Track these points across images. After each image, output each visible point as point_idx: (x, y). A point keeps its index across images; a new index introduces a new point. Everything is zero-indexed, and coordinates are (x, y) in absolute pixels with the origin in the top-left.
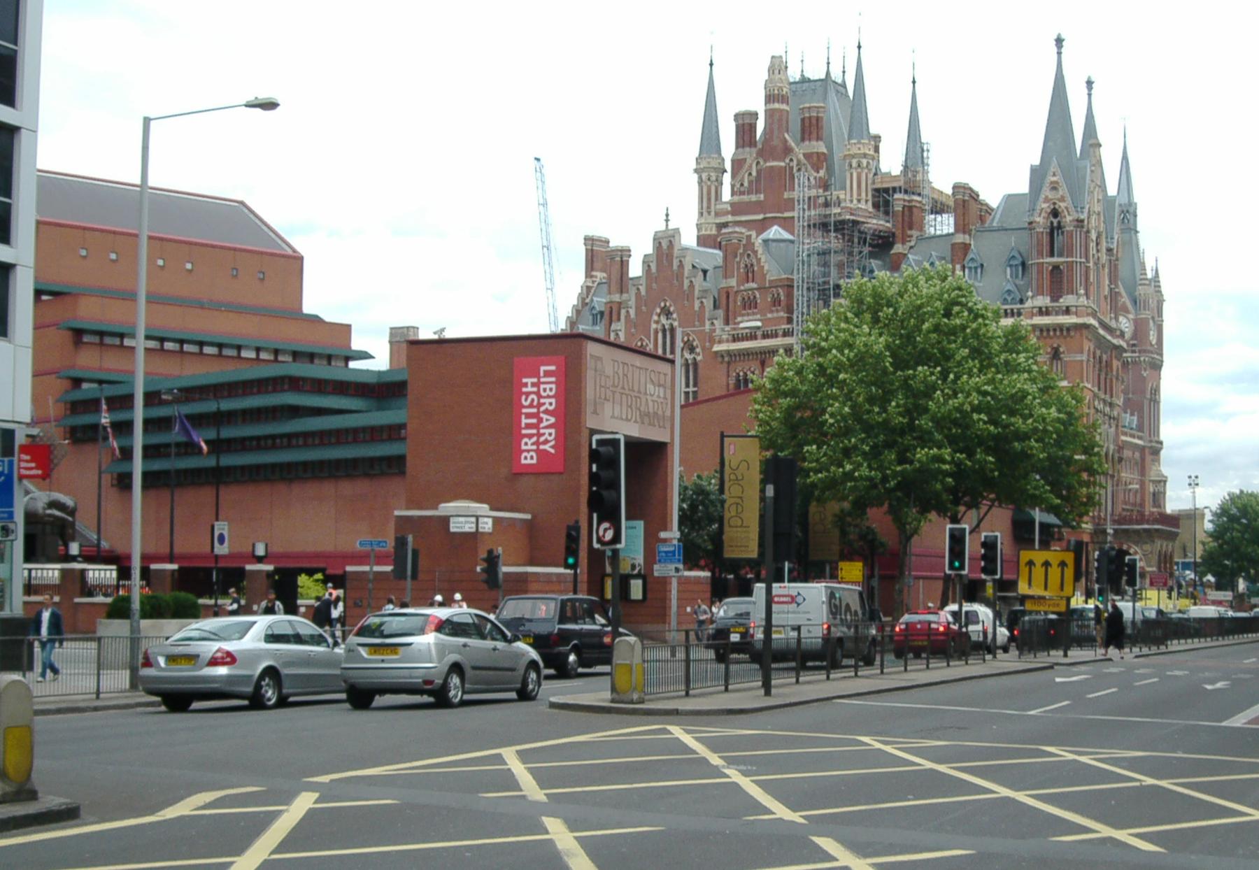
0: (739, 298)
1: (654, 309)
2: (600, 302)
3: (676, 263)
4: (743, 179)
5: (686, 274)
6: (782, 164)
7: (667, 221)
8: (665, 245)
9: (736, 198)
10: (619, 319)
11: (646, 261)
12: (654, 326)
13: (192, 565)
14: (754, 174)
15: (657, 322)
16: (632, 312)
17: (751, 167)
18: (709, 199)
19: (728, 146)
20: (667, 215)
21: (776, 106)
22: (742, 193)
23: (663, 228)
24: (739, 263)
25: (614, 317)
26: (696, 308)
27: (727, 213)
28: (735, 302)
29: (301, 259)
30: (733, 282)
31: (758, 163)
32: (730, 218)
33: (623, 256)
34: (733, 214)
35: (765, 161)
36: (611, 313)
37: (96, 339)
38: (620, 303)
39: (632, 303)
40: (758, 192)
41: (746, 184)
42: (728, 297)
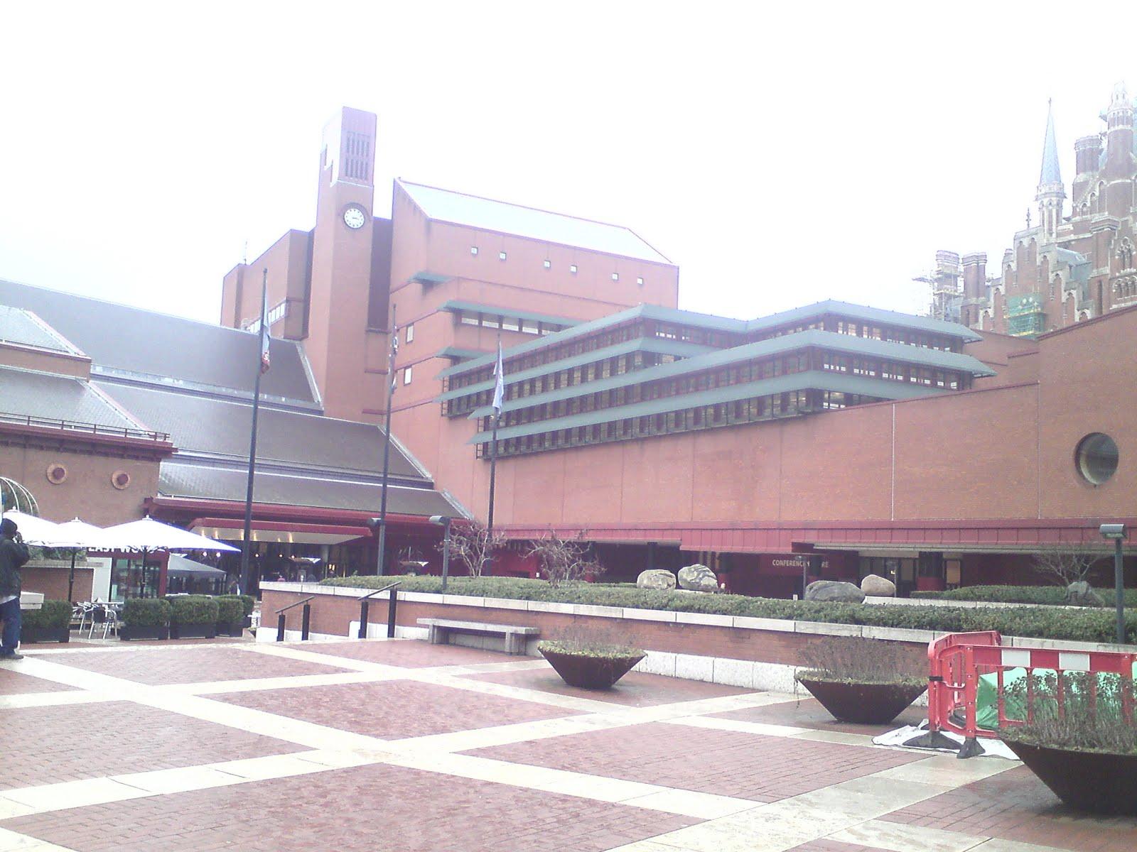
0: (1114, 285)
3: (1039, 259)
4: (1085, 200)
5: (1051, 268)
6: (1129, 181)
8: (1026, 242)
9: (1078, 218)
10: (977, 321)
14: (1097, 194)
17: (1093, 189)
18: (1050, 223)
19: (1069, 175)
20: (1028, 215)
21: (1121, 127)
22: (1083, 213)
24: (1114, 249)
25: (972, 319)
26: (1064, 300)
27: (1072, 232)
28: (1109, 289)
30: (1107, 270)
31: (1102, 183)
32: (1072, 237)
33: (977, 264)
34: (1075, 232)
35: (1108, 182)
37: (475, 322)
38: (977, 307)
40: (1101, 210)
41: (1088, 204)
42: (1101, 285)
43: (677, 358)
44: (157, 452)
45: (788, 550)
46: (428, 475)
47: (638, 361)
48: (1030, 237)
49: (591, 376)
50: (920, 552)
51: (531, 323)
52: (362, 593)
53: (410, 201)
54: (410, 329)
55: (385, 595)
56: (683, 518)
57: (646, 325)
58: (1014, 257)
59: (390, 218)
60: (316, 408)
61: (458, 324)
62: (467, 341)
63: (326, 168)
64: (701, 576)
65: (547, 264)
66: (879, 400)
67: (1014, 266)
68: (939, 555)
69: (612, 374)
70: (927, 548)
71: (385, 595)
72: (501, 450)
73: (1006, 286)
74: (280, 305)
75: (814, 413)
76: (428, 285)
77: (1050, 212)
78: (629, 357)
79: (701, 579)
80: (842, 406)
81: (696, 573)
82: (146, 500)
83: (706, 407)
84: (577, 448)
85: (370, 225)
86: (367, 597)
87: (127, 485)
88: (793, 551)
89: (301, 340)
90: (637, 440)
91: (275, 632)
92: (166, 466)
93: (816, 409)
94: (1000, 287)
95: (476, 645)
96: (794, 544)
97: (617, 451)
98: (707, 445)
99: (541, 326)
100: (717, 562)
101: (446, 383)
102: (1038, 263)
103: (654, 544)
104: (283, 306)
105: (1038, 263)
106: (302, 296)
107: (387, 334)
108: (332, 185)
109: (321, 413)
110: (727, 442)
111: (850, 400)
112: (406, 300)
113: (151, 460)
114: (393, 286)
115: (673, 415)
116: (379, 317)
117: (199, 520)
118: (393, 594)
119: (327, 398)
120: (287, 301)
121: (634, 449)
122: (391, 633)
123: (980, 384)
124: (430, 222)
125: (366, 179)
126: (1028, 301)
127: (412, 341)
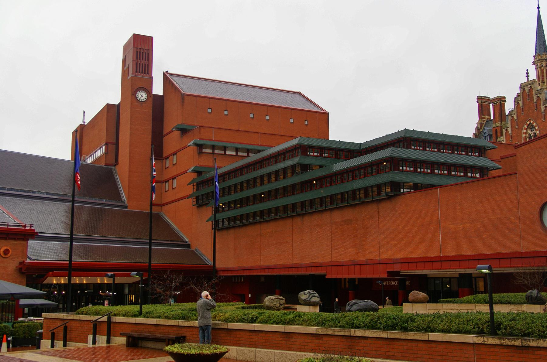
1: (523, 126)
2: (487, 130)
3: (535, 98)
7: (528, 76)
8: (527, 89)
10: (502, 135)
11: (516, 100)
12: (524, 135)
13: (251, 274)
15: (526, 133)
16: (509, 130)
20: (527, 73)
23: (525, 80)
25: (499, 134)
29: (328, 114)
33: (500, 101)
36: (496, 132)
37: (210, 151)
38: (501, 127)
39: (509, 125)
43: (321, 167)
44: (26, 234)
45: (385, 276)
46: (187, 240)
47: (298, 169)
48: (529, 86)
49: (273, 179)
50: (459, 274)
51: (243, 150)
52: (93, 318)
53: (173, 84)
54: (175, 157)
55: (105, 319)
56: (326, 259)
57: (303, 149)
58: (520, 98)
59: (161, 93)
60: (123, 204)
61: (200, 153)
62: (206, 162)
63: (125, 68)
64: (311, 296)
65: (252, 116)
66: (433, 186)
67: (521, 103)
68: (471, 274)
69: (284, 178)
70: (462, 271)
71: (105, 319)
72: (226, 224)
73: (517, 115)
74: (102, 147)
75: (395, 196)
76: (184, 131)
77: (542, 70)
78: (293, 167)
79: (311, 298)
80: (412, 191)
81: (308, 295)
82: (21, 263)
83: (336, 195)
84: (267, 221)
85: (151, 99)
86: (96, 321)
87: (9, 255)
88: (388, 276)
89: (115, 166)
90: (299, 215)
91: (49, 341)
92: (30, 242)
93: (397, 193)
94: (513, 115)
95: (152, 347)
96: (388, 272)
97: (289, 222)
98: (337, 216)
99: (248, 151)
100: (347, 284)
101: (195, 187)
102: (535, 101)
103: (313, 275)
104: (104, 147)
105: (535, 101)
106: (114, 141)
107: (162, 160)
108: (128, 78)
109: (126, 207)
110: (349, 214)
111: (416, 187)
112: (172, 141)
113: (23, 240)
114: (165, 133)
115: (319, 199)
116: (158, 151)
117: (51, 273)
118: (109, 318)
119: (128, 198)
120: (107, 144)
121: (298, 220)
122: (108, 341)
123: (493, 173)
124: (183, 96)
125: (148, 73)
126: (530, 123)
127: (175, 164)
